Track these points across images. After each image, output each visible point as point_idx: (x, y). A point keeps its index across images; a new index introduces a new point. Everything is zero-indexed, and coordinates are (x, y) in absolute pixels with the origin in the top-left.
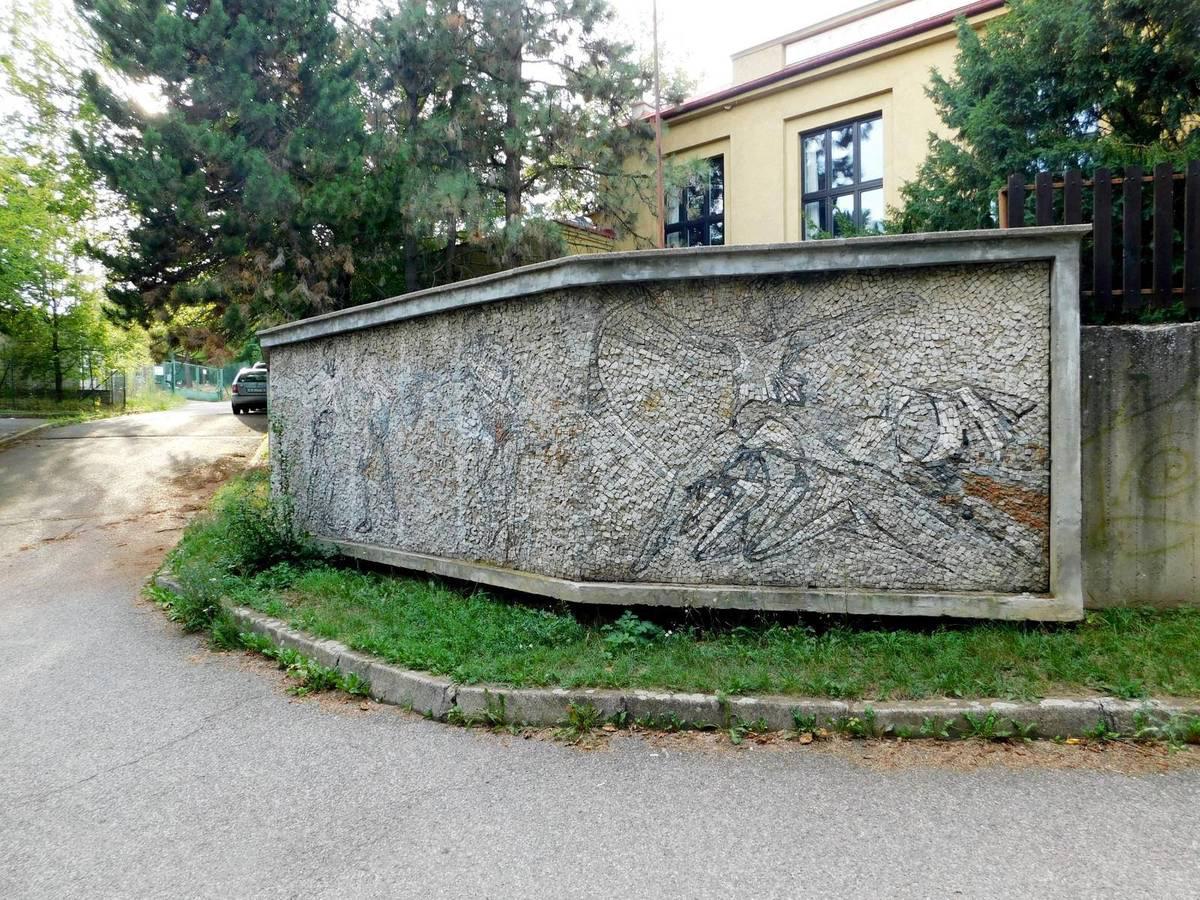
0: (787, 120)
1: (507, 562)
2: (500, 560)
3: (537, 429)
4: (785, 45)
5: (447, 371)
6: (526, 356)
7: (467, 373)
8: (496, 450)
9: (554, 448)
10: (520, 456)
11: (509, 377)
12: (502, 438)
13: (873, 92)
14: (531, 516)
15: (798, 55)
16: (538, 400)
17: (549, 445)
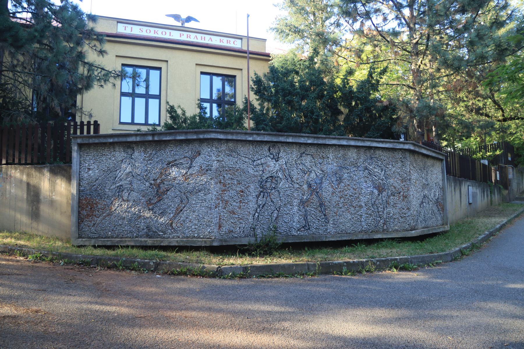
0: (116, 56)
1: (384, 230)
2: (381, 230)
3: (395, 188)
4: (118, 22)
5: (355, 167)
6: (390, 166)
7: (366, 168)
8: (379, 195)
9: (402, 193)
10: (389, 197)
11: (383, 172)
12: (380, 192)
13: (160, 59)
14: (393, 214)
15: (121, 29)
16: (396, 179)
17: (400, 193)
